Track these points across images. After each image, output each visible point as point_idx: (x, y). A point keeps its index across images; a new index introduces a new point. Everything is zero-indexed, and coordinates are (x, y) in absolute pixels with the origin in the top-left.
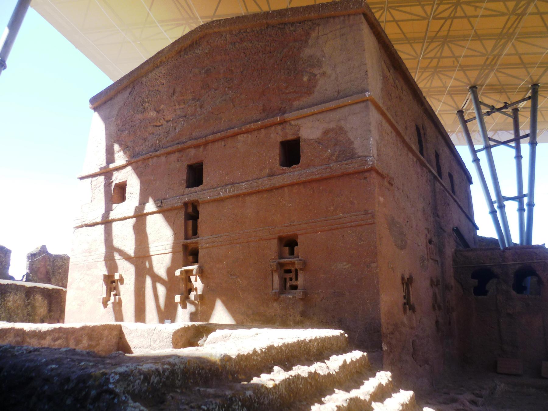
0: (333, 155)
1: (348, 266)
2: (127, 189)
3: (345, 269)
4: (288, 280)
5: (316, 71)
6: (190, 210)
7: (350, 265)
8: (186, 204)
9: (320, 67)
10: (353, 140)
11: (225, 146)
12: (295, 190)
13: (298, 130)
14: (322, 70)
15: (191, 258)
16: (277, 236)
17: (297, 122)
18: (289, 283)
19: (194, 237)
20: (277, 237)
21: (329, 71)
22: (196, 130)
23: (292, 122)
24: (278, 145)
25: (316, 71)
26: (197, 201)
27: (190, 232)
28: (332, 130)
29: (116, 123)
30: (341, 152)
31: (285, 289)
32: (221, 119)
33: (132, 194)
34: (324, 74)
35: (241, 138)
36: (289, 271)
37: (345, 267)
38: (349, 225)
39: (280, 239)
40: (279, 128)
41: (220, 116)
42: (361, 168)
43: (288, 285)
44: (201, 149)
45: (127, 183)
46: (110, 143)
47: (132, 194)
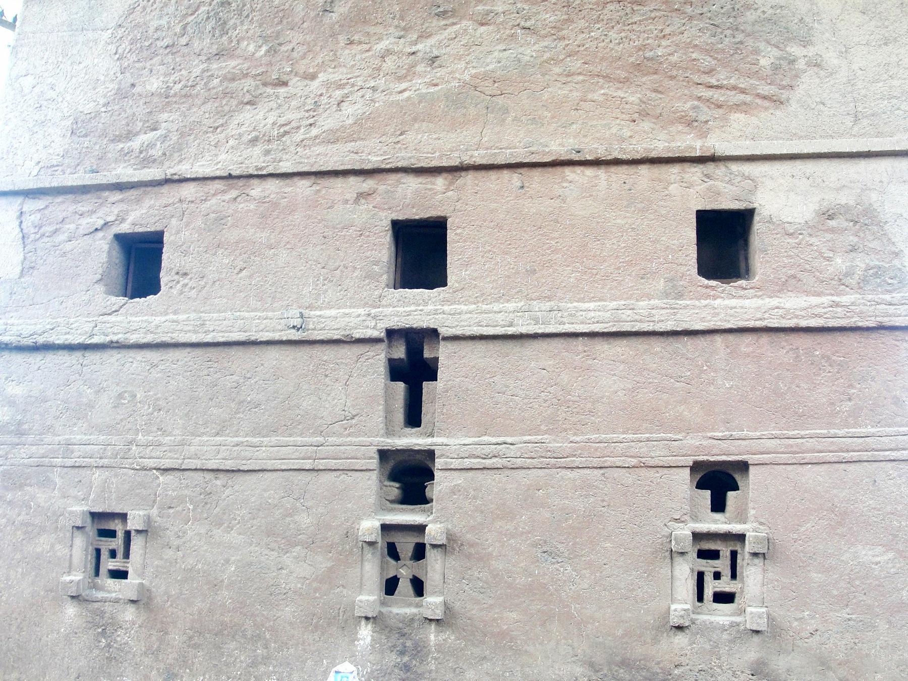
1: (886, 558)
2: (164, 257)
3: (877, 564)
4: (708, 578)
5: (795, 50)
6: (400, 352)
7: (891, 555)
8: (391, 333)
11: (522, 187)
12: (746, 343)
13: (752, 192)
14: (811, 51)
15: (394, 490)
18: (711, 586)
19: (409, 430)
20: (691, 464)
21: (831, 58)
22: (416, 126)
25: (795, 50)
26: (433, 333)
27: (399, 416)
28: (846, 208)
29: (112, 48)
30: (871, 271)
31: (700, 598)
32: (506, 111)
33: (186, 274)
36: (714, 555)
37: (878, 559)
39: (696, 467)
41: (500, 100)
43: (708, 593)
45: (166, 239)
46: (92, 104)
47: (186, 274)
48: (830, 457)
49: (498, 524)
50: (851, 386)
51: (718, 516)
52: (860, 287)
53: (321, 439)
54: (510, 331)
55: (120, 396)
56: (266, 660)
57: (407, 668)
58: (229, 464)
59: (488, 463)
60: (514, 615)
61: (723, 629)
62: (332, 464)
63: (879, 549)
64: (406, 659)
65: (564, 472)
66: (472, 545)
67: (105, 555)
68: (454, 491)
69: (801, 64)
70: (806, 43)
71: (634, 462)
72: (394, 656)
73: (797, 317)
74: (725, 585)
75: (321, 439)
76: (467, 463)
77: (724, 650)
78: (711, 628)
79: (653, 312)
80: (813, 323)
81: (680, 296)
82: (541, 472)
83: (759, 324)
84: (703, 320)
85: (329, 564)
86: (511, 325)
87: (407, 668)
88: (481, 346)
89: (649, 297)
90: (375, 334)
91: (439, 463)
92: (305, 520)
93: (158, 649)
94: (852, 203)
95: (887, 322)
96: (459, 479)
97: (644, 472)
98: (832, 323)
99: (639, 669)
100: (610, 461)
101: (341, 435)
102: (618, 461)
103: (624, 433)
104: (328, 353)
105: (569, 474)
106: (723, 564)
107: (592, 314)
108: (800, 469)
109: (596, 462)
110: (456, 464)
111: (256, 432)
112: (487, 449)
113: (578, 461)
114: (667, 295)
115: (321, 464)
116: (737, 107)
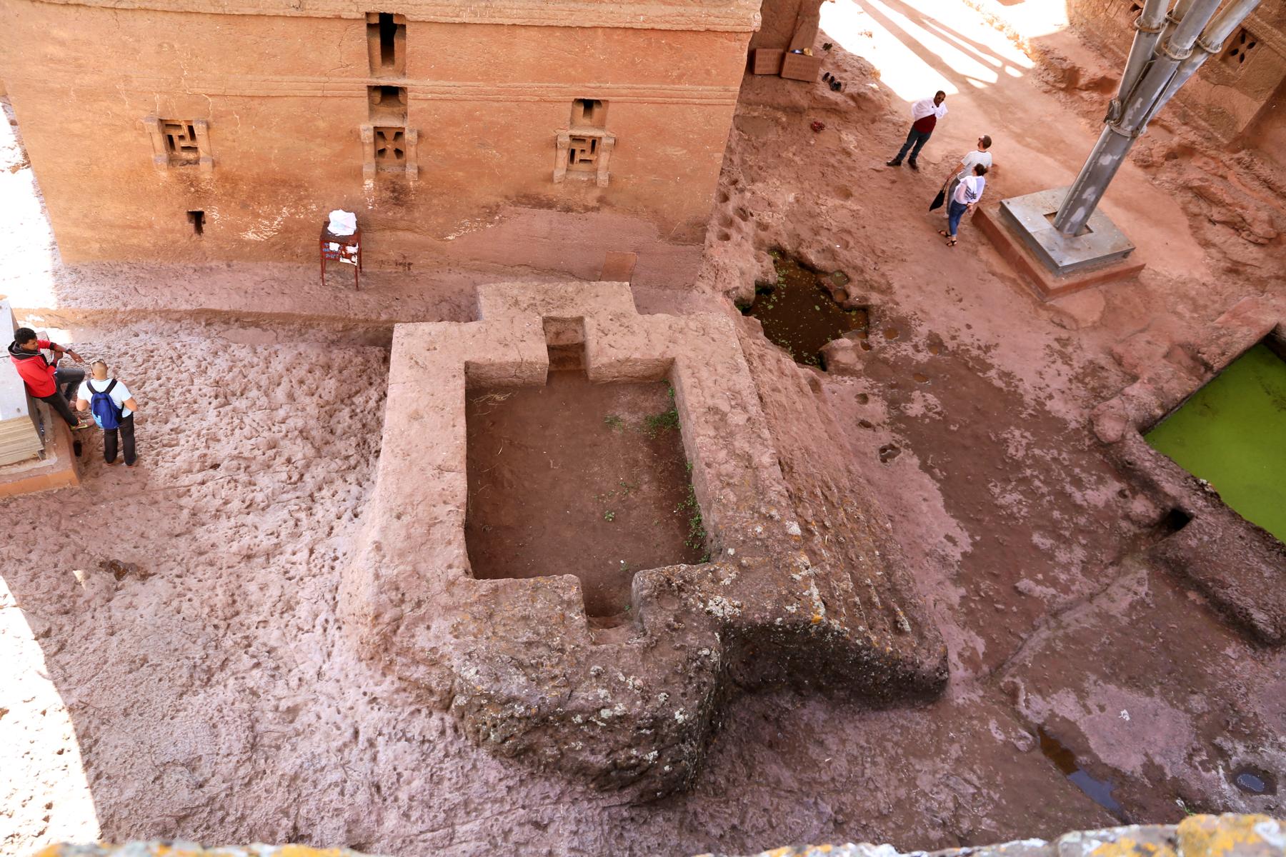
7: (685, 151)
12: (616, 36)
16: (573, 98)
18: (578, 156)
38: (697, 101)
42: (738, 29)
48: (660, 100)
49: (451, 129)
50: (681, 62)
51: (587, 121)
53: (326, 79)
54: (458, 20)
55: (160, 46)
56: (307, 197)
58: (261, 93)
59: (443, 96)
60: (461, 174)
61: (583, 181)
62: (337, 93)
63: (679, 148)
65: (491, 103)
66: (434, 139)
67: (176, 140)
68: (421, 110)
71: (537, 98)
72: (388, 193)
73: (653, 22)
74: (586, 156)
75: (326, 79)
76: (430, 96)
77: (583, 191)
78: (578, 181)
79: (557, 12)
80: (663, 27)
82: (478, 103)
83: (628, 25)
84: (591, 20)
85: (341, 147)
86: (457, 16)
88: (436, 27)
90: (359, 16)
91: (410, 95)
92: (322, 124)
93: (233, 193)
95: (712, 28)
96: (425, 105)
97: (543, 104)
98: (676, 28)
99: (534, 199)
100: (522, 98)
101: (340, 76)
102: (527, 98)
103: (533, 82)
104: (323, 25)
105: (496, 104)
106: (587, 146)
107: (515, 11)
108: (640, 105)
109: (513, 98)
110: (421, 96)
111: (277, 73)
112: (443, 89)
113: (501, 97)
115: (329, 93)
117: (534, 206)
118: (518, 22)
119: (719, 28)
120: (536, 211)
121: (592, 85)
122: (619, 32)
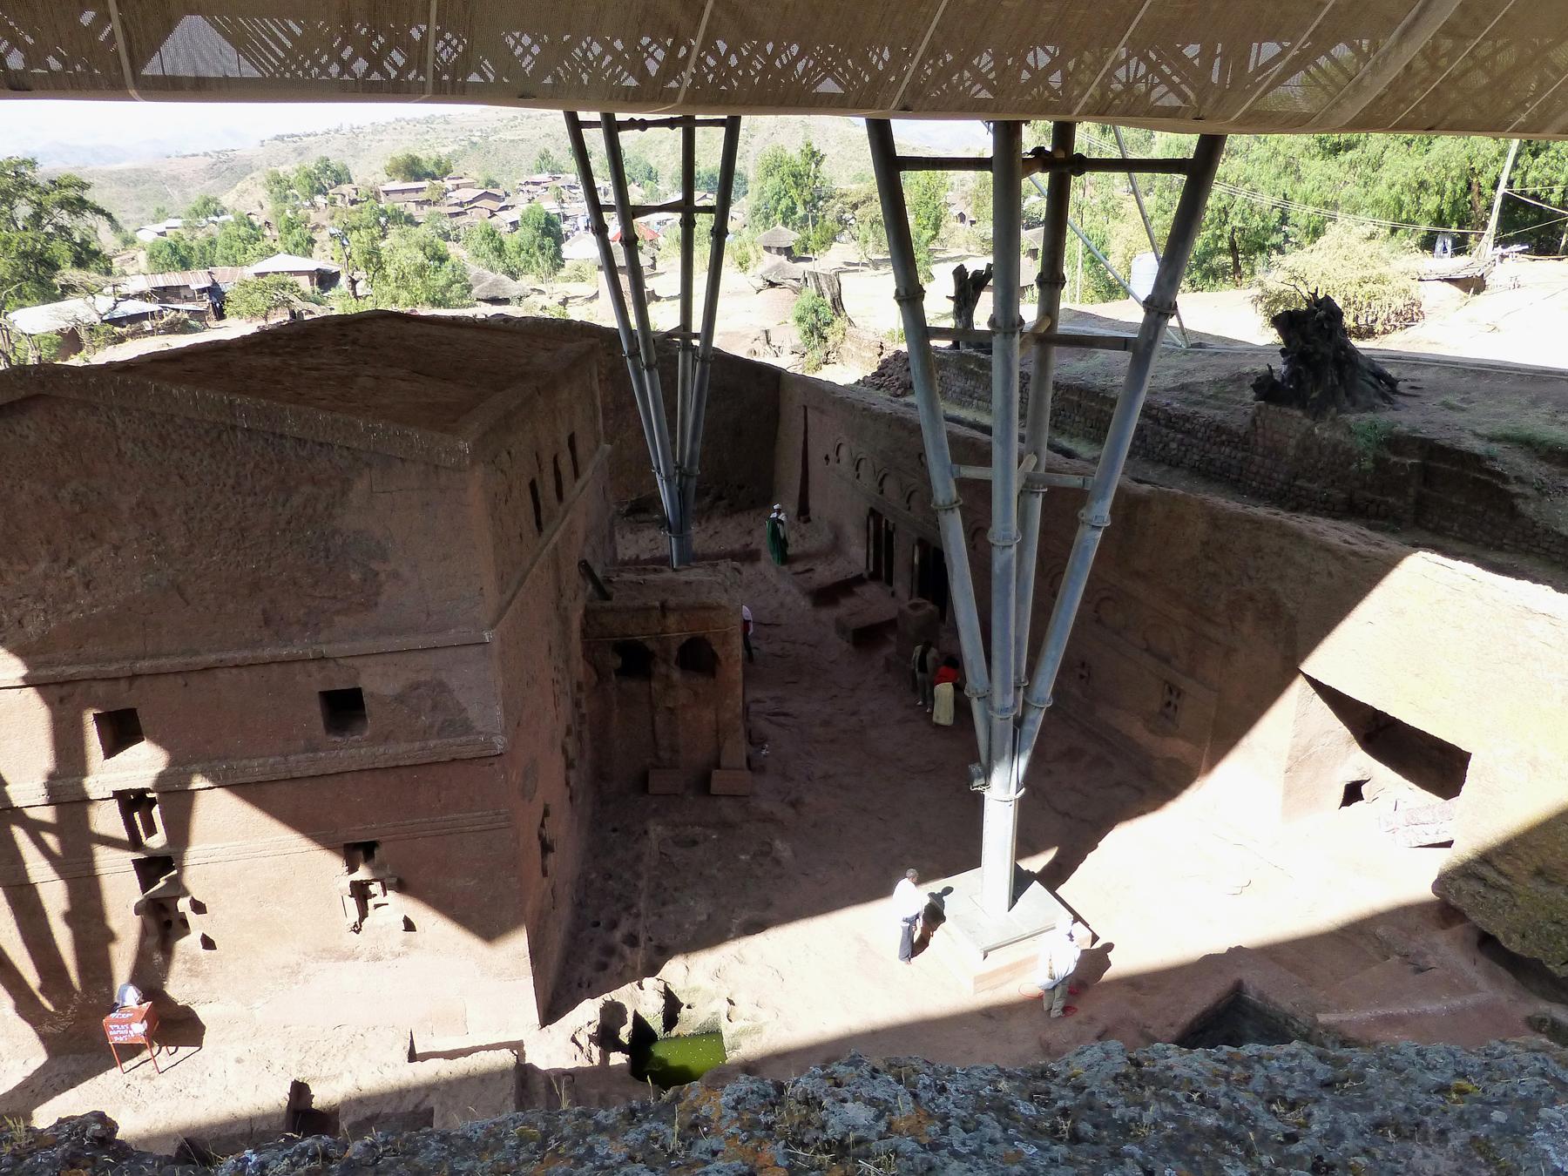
0: (431, 726)
5: (374, 565)
7: (475, 881)
9: (385, 560)
10: (465, 705)
11: (186, 685)
17: (350, 662)
22: (90, 641)
23: (342, 661)
24: (317, 696)
28: (426, 683)
34: (396, 575)
35: (222, 675)
38: (472, 829)
40: (313, 667)
42: (485, 753)
44: (123, 685)
52: (439, 735)
57: (190, 970)
64: (188, 966)
69: (383, 577)
70: (385, 560)
81: (316, 750)
87: (190, 970)
89: (296, 753)
94: (429, 679)
95: (457, 756)
113: (268, 853)
114: (306, 751)
116: (338, 612)
117: (338, 959)
118: (260, 778)
119: (464, 756)
120: (341, 964)
121: (357, 828)
122: (367, 773)
